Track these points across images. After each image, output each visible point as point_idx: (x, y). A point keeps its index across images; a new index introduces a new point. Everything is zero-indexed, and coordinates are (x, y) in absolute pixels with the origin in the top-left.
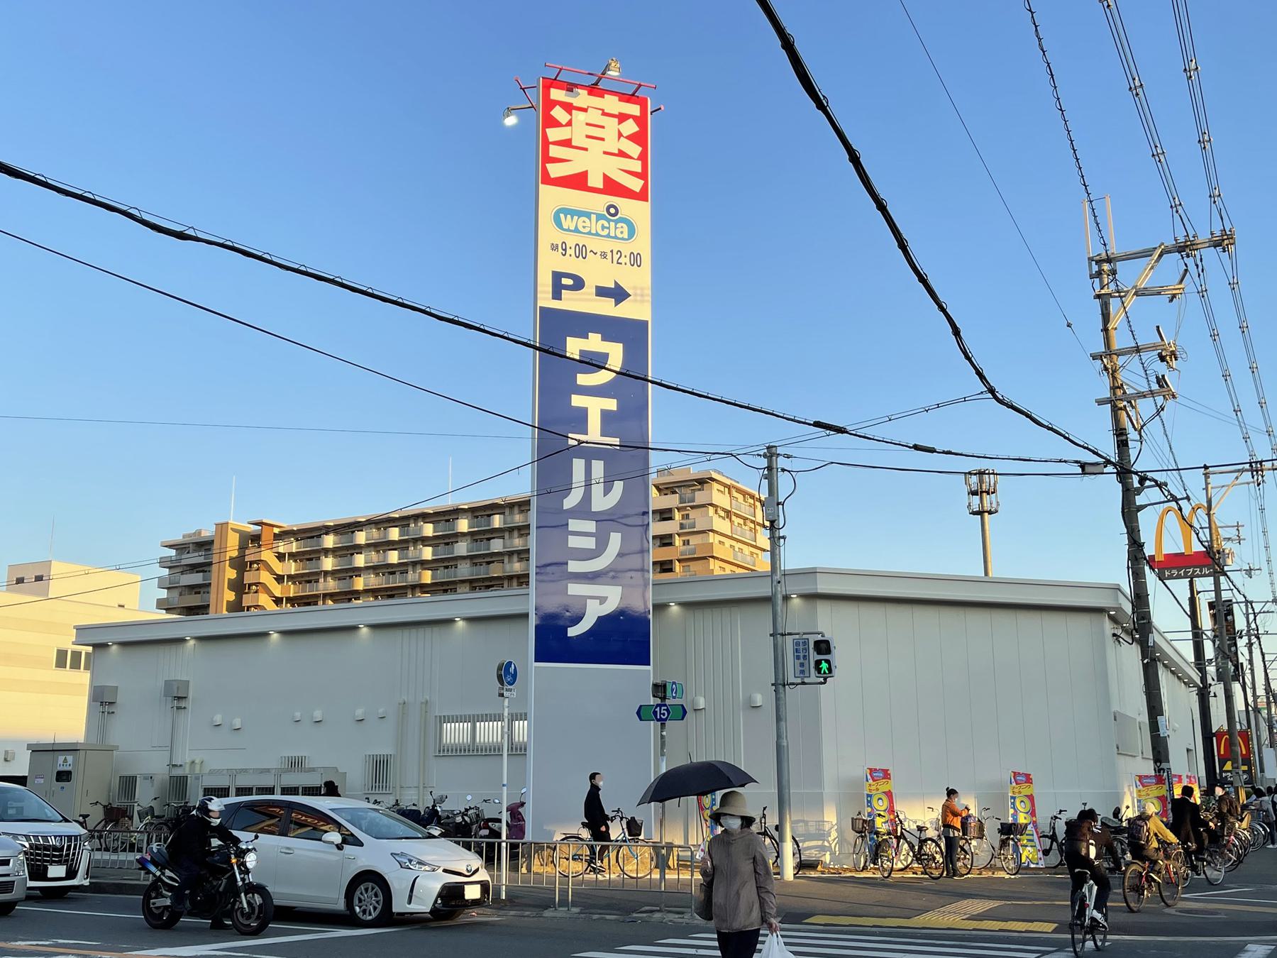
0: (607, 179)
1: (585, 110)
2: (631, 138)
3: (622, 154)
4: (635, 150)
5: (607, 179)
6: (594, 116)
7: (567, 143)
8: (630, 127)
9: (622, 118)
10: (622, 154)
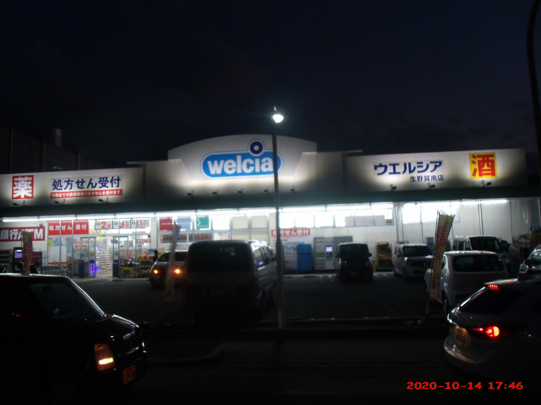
3: (28, 189)
4: (30, 187)
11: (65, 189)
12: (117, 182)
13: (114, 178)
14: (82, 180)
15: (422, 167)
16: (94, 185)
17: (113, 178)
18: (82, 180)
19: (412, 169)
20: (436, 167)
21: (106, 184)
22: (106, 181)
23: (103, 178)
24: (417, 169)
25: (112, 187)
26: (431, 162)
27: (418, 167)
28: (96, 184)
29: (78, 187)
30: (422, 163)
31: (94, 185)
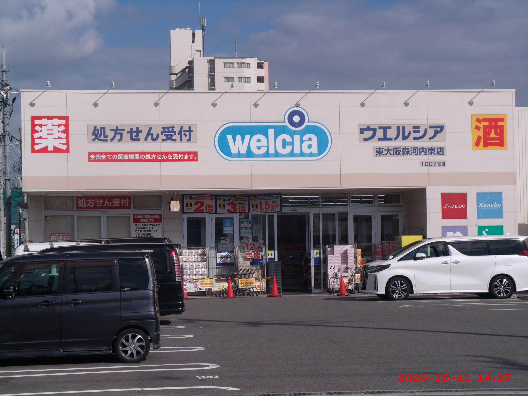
0: (54, 147)
1: (46, 125)
2: (63, 132)
3: (59, 138)
4: (64, 136)
5: (54, 147)
6: (50, 127)
7: (41, 138)
8: (62, 128)
9: (59, 125)
10: (59, 138)
11: (112, 140)
12: (187, 133)
13: (184, 129)
14: (138, 128)
15: (419, 132)
16: (155, 137)
17: (182, 127)
18: (138, 128)
19: (407, 134)
20: (436, 133)
21: (172, 136)
22: (172, 131)
23: (168, 128)
24: (413, 135)
25: (181, 140)
26: (431, 127)
27: (414, 132)
28: (158, 135)
29: (132, 139)
30: (418, 127)
31: (155, 137)
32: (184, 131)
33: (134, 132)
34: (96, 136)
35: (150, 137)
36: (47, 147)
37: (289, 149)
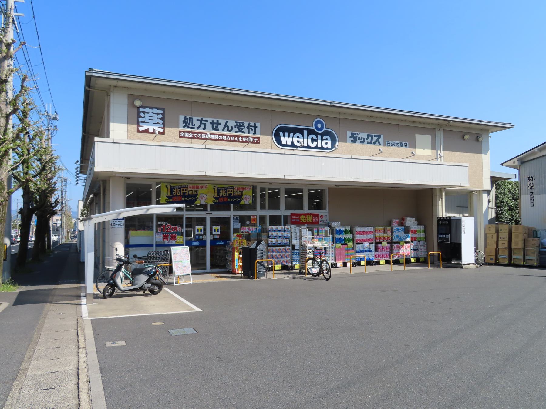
3: (158, 123)
4: (161, 122)
6: (151, 114)
8: (160, 116)
9: (158, 114)
12: (253, 128)
16: (230, 129)
21: (242, 129)
22: (243, 126)
23: (240, 123)
31: (230, 129)
32: (251, 126)
33: (215, 123)
34: (186, 124)
35: (226, 128)
36: (148, 129)
37: (315, 143)
